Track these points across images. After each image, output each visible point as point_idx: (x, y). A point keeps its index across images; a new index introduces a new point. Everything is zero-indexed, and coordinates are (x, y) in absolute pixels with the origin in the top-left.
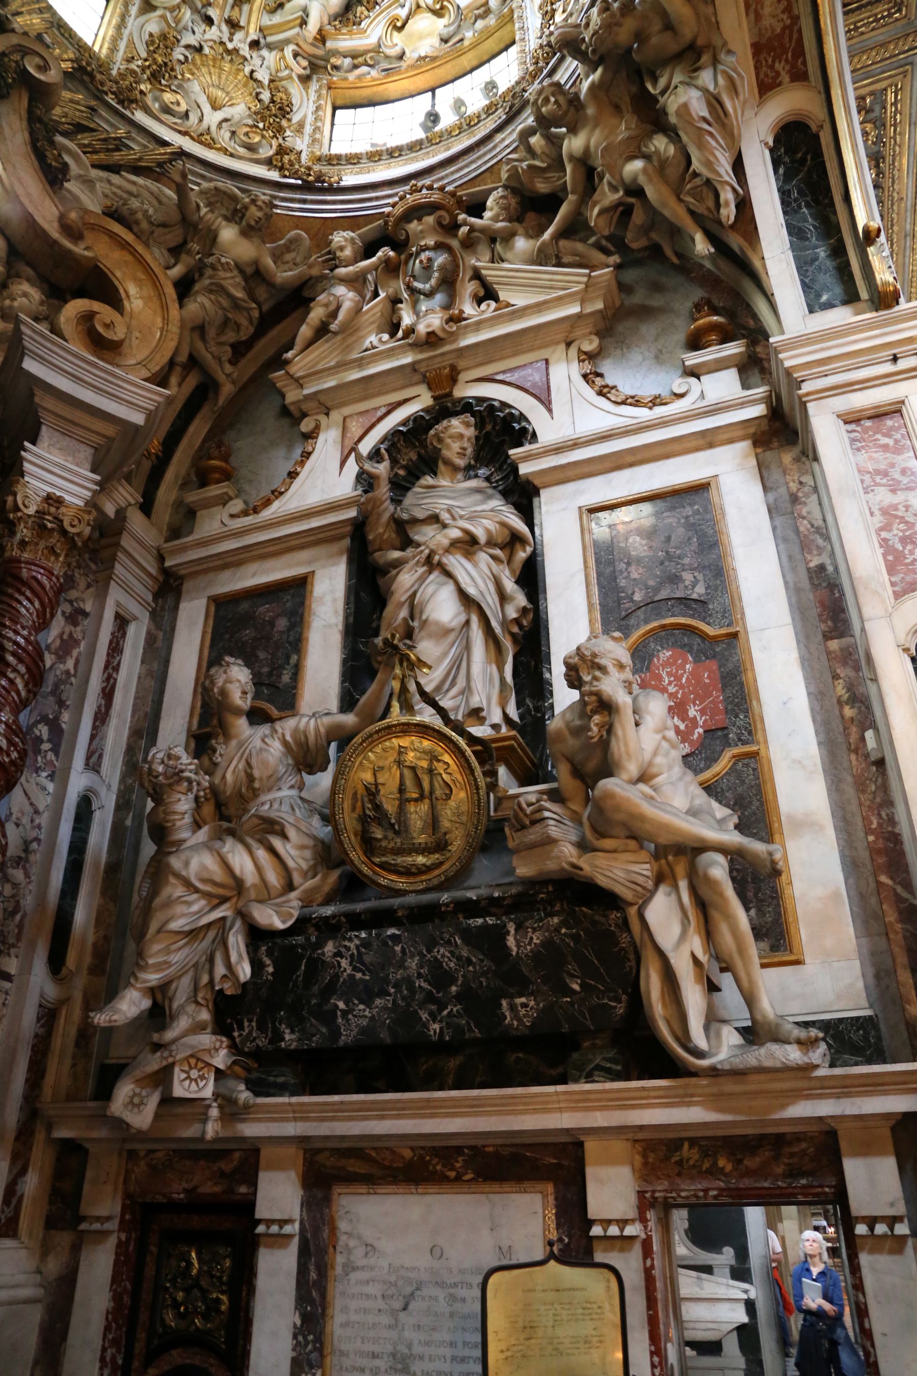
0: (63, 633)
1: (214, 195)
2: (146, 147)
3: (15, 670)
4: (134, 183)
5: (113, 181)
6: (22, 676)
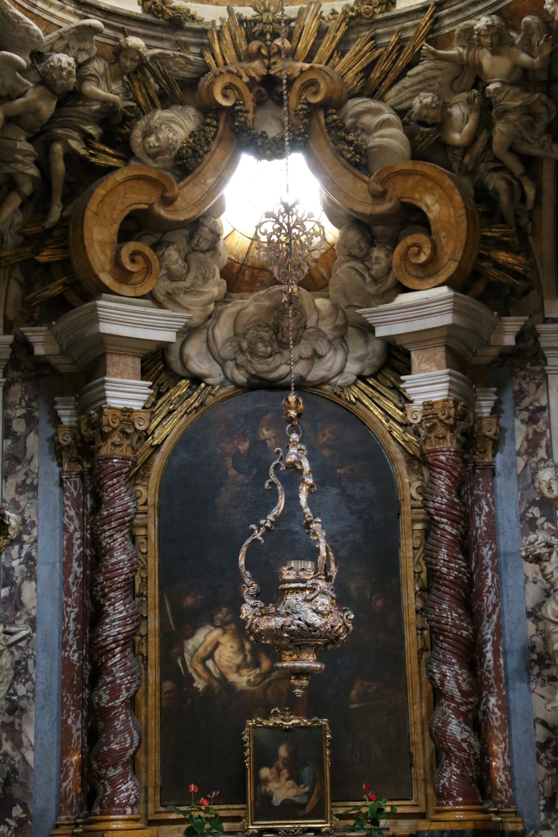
0: (528, 435)
1: (465, 35)
2: (416, 25)
3: (442, 523)
4: (418, 74)
5: (407, 85)
6: (447, 524)
